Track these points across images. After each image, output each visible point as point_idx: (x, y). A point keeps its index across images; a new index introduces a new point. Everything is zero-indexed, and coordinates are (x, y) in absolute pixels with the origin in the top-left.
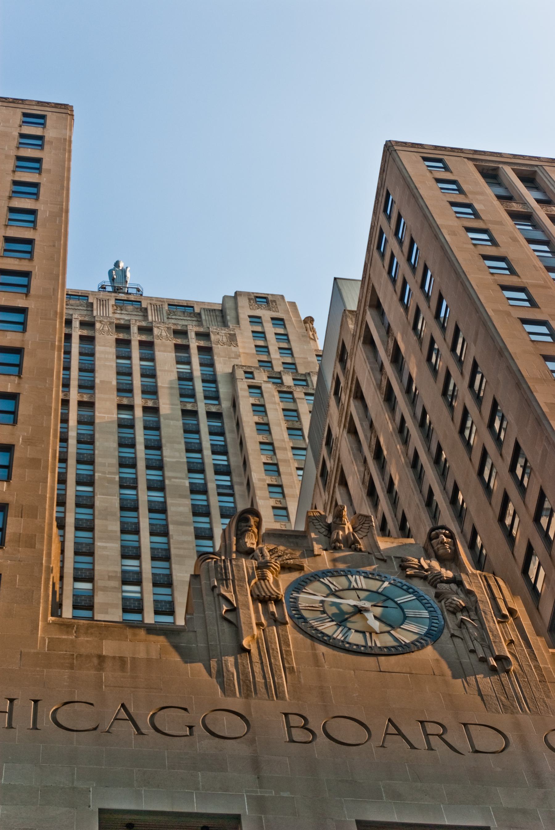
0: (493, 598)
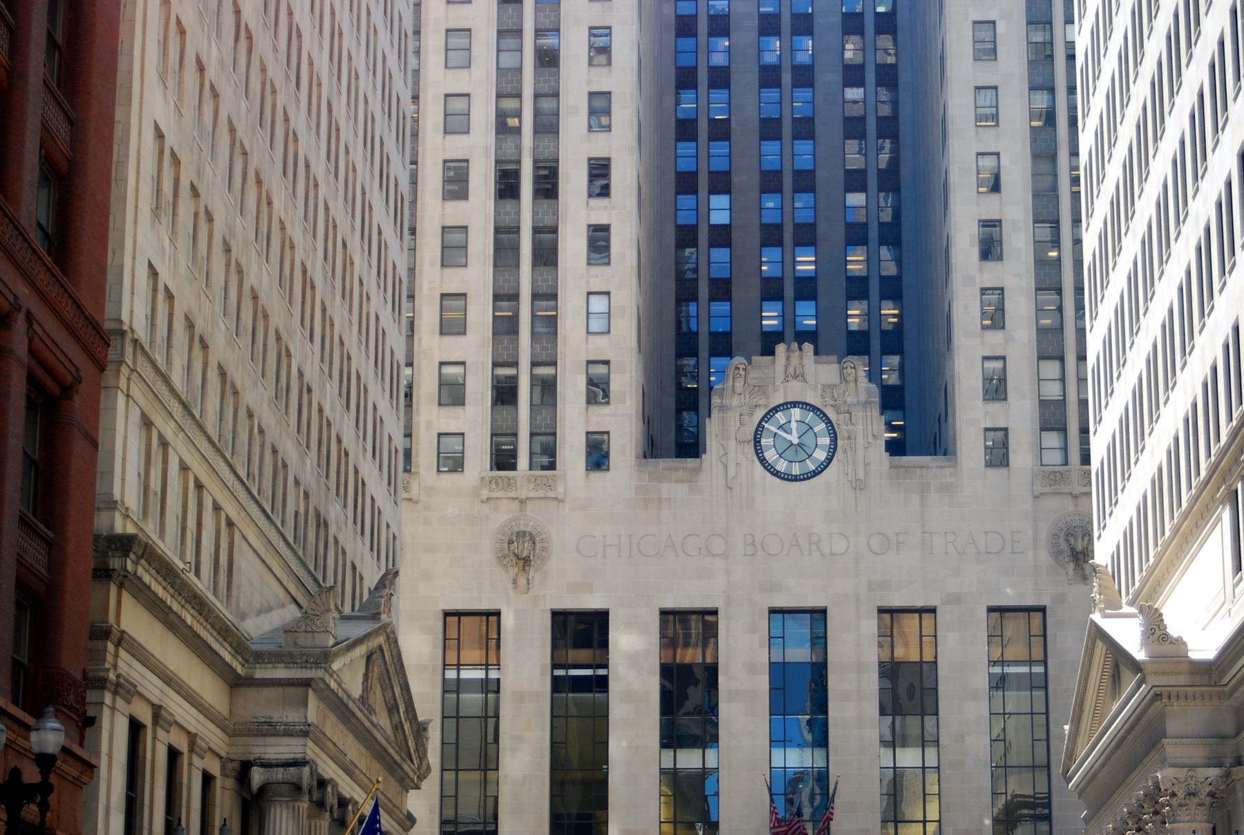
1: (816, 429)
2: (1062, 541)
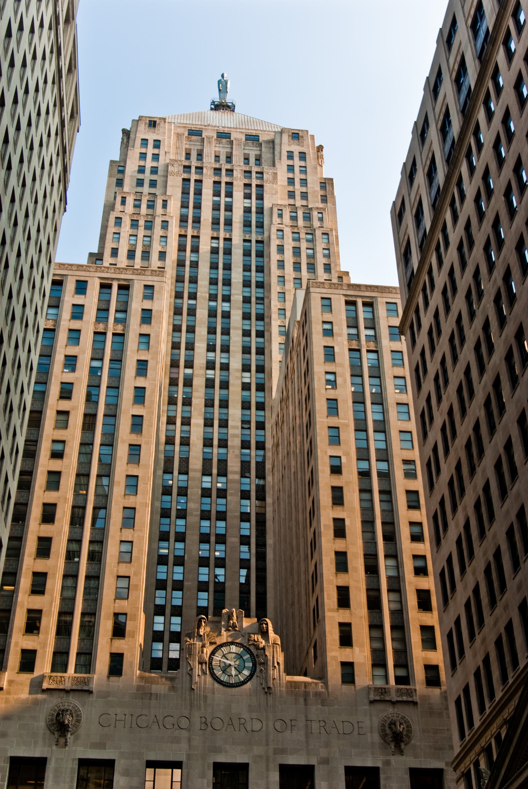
0: (273, 658)
1: (245, 658)
2: (387, 728)
